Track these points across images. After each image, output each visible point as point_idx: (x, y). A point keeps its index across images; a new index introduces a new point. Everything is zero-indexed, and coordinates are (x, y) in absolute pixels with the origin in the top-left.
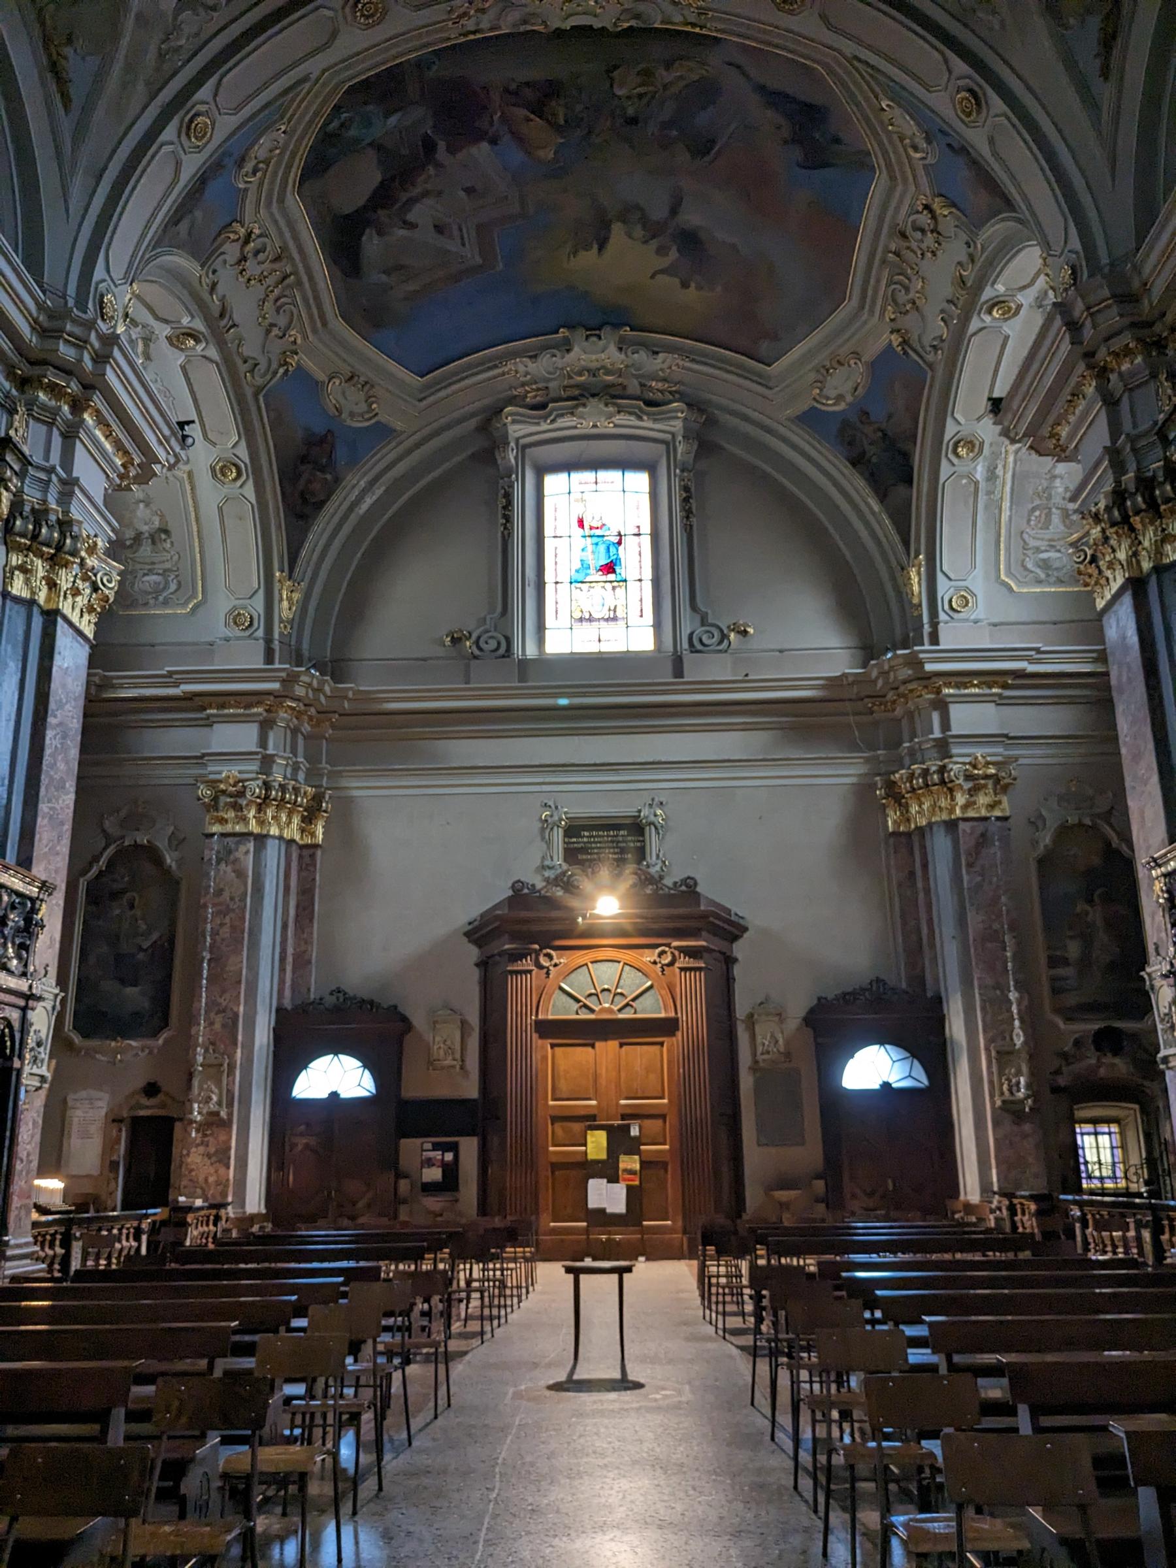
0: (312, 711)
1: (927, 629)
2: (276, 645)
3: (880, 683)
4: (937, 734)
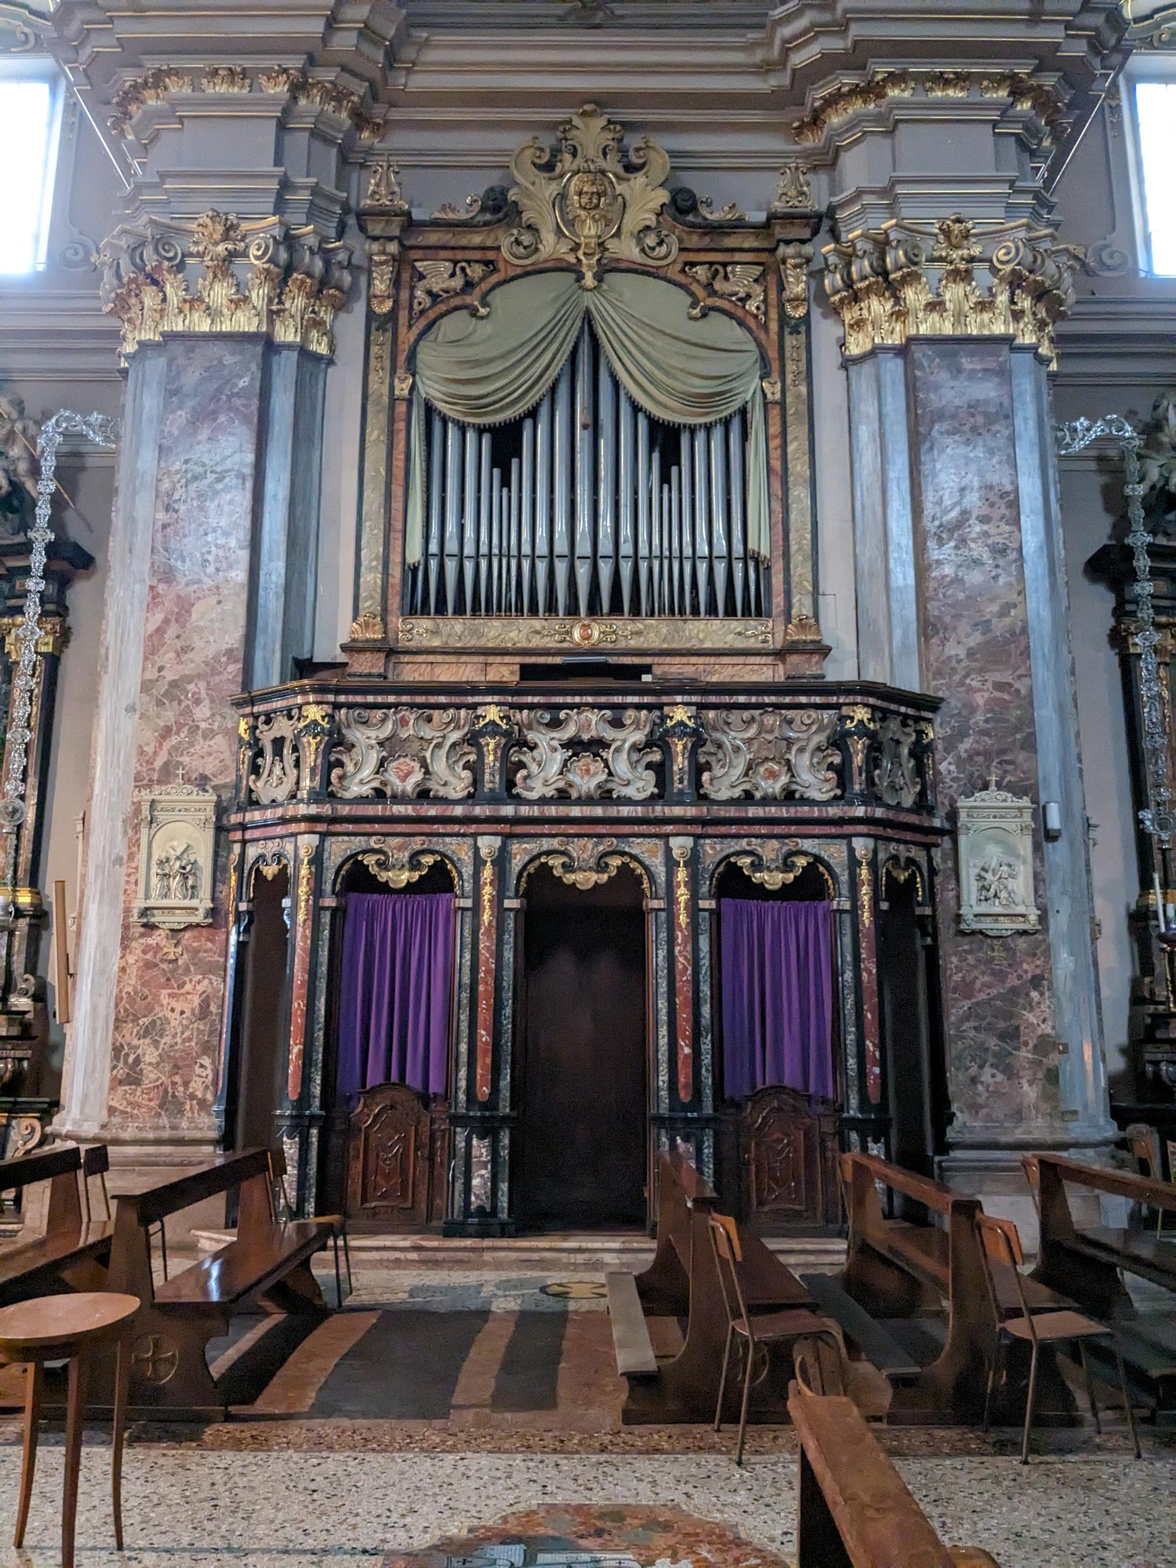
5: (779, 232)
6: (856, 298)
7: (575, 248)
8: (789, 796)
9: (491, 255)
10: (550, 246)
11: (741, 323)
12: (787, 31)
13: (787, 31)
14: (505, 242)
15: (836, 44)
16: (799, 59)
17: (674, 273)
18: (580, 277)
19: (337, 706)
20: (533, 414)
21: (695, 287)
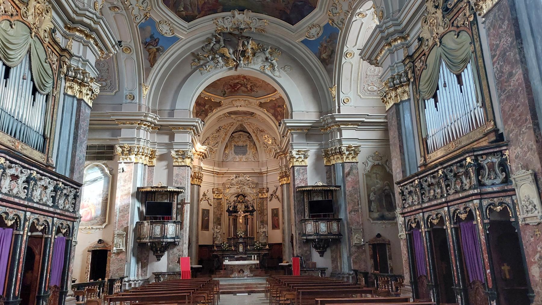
0: (153, 125)
4: (339, 138)
6: (73, 81)
8: (68, 211)
10: (30, 19)
11: (52, 70)
12: (88, 13)
13: (88, 13)
17: (45, 46)
19: (6, 159)
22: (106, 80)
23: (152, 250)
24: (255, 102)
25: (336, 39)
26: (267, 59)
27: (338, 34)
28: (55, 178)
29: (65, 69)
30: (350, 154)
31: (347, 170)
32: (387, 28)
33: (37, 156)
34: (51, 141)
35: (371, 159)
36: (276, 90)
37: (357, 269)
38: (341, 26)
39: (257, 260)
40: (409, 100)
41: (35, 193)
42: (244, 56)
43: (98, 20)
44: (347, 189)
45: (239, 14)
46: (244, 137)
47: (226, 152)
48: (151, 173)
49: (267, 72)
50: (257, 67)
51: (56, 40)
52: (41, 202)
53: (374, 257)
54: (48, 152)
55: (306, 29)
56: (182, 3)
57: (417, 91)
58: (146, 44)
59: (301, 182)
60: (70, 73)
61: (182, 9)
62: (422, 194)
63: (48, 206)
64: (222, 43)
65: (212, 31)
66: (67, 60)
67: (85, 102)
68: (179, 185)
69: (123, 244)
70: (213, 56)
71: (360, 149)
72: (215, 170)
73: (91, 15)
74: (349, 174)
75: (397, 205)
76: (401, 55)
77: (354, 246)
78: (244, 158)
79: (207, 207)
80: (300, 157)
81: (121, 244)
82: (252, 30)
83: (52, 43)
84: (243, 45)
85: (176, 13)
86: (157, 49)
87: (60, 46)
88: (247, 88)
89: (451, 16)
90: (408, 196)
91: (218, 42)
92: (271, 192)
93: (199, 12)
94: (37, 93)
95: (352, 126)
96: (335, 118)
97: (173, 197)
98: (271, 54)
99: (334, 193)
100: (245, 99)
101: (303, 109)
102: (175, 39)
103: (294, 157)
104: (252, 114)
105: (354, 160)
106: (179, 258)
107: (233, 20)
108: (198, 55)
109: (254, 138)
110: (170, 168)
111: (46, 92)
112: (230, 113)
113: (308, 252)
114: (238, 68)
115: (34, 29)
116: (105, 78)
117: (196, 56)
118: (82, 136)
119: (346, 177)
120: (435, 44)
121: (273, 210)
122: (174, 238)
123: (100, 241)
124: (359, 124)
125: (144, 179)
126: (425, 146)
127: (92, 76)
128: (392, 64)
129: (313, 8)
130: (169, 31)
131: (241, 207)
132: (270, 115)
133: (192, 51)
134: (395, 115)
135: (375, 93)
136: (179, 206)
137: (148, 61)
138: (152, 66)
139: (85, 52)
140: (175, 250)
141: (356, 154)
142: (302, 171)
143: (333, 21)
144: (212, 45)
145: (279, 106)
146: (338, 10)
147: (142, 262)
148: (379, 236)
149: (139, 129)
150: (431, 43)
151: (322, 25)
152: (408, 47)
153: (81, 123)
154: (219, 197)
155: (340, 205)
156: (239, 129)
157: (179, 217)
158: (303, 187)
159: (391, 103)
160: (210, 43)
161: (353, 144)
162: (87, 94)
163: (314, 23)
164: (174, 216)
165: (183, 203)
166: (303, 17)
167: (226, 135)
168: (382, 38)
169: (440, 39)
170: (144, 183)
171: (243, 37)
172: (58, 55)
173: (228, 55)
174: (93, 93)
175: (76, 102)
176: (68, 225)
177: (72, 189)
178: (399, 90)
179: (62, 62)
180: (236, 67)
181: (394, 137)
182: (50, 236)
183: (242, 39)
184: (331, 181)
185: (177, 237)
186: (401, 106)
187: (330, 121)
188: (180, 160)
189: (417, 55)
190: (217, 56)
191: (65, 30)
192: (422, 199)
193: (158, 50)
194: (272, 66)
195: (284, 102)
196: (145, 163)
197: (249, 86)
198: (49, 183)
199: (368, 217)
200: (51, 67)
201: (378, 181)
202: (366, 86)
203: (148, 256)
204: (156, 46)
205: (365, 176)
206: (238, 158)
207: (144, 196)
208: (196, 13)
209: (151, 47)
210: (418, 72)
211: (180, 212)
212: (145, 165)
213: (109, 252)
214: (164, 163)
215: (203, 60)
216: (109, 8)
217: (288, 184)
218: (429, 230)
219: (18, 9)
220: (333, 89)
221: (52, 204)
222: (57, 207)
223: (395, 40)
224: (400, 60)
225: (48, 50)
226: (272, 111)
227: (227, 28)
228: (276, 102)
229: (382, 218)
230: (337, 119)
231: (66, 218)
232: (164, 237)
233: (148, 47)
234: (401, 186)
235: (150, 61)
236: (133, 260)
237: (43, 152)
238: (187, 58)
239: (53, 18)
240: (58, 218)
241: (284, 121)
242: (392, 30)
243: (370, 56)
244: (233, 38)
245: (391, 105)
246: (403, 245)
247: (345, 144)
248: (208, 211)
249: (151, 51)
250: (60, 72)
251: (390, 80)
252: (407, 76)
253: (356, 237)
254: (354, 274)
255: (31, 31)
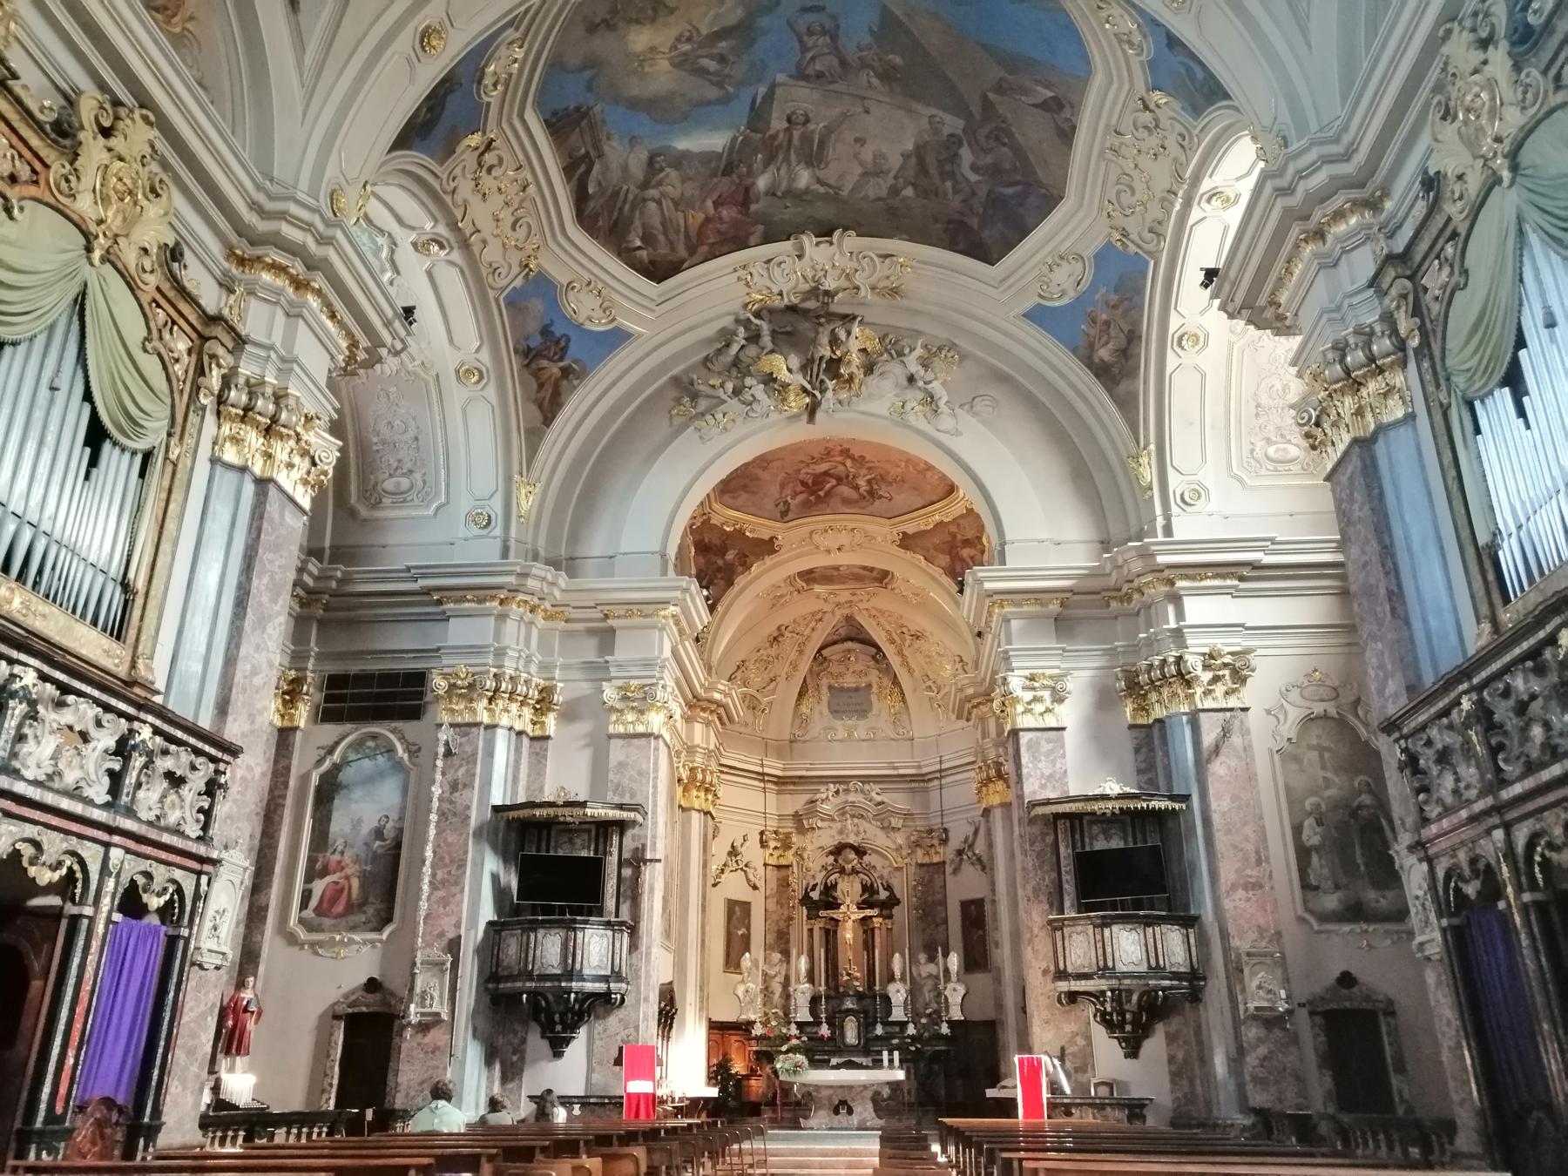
0: (547, 605)
1: (1160, 522)
2: (512, 542)
3: (1114, 575)
4: (1172, 625)
5: (218, 331)
6: (243, 419)
7: (100, 222)
8: (181, 834)
9: (38, 166)
10: (85, 205)
13: (294, 209)
14: (55, 167)
15: (312, 245)
16: (288, 231)
18: (89, 249)
20: (14, 344)
21: (152, 325)
22: (411, 471)
23: (537, 1020)
24: (884, 532)
25: (1140, 291)
26: (911, 379)
27: (1145, 277)
28: (122, 706)
29: (214, 379)
30: (1216, 679)
31: (1208, 739)
32: (1300, 175)
33: (90, 644)
34: (152, 603)
35: (1294, 695)
36: (951, 489)
37: (1267, 1106)
38: (1150, 247)
39: (901, 1067)
40: (1410, 418)
41: (27, 748)
42: (836, 376)
43: (329, 232)
44: (1214, 805)
45: (817, 244)
46: (860, 658)
47: (804, 709)
48: (539, 759)
49: (912, 419)
50: (881, 407)
51: (188, 285)
52: (56, 785)
53: (1333, 1059)
54: (137, 640)
55: (1036, 272)
56: (637, 223)
57: (1438, 376)
58: (529, 356)
59: (1043, 787)
60: (233, 393)
61: (638, 243)
62: (1494, 751)
63: (89, 802)
64: (766, 340)
65: (736, 305)
66: (221, 351)
67: (281, 490)
68: (626, 800)
69: (441, 996)
70: (739, 383)
71: (1254, 661)
72: (767, 770)
73: (304, 214)
74: (1216, 750)
75: (1397, 823)
76: (1364, 263)
77: (1254, 1018)
78: (861, 728)
79: (743, 894)
80: (1036, 699)
81: (436, 994)
82: (863, 293)
83: (171, 294)
84: (834, 341)
85: (619, 255)
86: (562, 369)
87: (199, 306)
88: (857, 488)
89: (1546, 55)
90: (1435, 770)
91: (754, 338)
92: (956, 841)
93: (692, 250)
94: (107, 446)
95: (1217, 582)
96: (1153, 555)
97: (607, 838)
98: (925, 366)
99: (1170, 824)
100: (851, 525)
101: (1043, 537)
102: (617, 338)
103: (1016, 700)
104: (882, 577)
105: (1233, 702)
106: (621, 1049)
107: (798, 265)
108: (692, 384)
109: (894, 661)
110: (600, 744)
111: (142, 445)
112: (809, 576)
113: (1081, 1042)
114: (819, 415)
115: (101, 240)
116: (409, 465)
117: (685, 388)
118: (265, 599)
119: (1209, 761)
120: (1494, 181)
121: (965, 905)
122: (605, 979)
123: (372, 985)
124: (1243, 574)
125: (515, 779)
126: (1491, 577)
127: (310, 408)
128: (1332, 301)
129: (1052, 200)
130: (598, 313)
131: (849, 890)
132: (937, 572)
133: (675, 372)
134: (1359, 481)
135: (1296, 468)
136: (627, 872)
137: (534, 408)
138: (548, 421)
139: (290, 337)
140: (613, 1021)
141: (1239, 677)
142: (1045, 747)
143: (1125, 234)
144: (735, 349)
145: (967, 543)
146: (1138, 196)
147: (505, 1059)
148: (1346, 979)
149: (502, 617)
150: (1474, 185)
151: (1088, 253)
152: (1391, 236)
153: (264, 554)
154: (783, 862)
155: (1194, 867)
156: (843, 632)
157: (625, 909)
158: (1048, 802)
159: (1344, 440)
160: (728, 346)
161: (1227, 644)
162: (290, 466)
163: (1063, 249)
164: (610, 903)
165: (638, 861)
166: (1022, 231)
167: (801, 652)
168: (1289, 217)
169: (1513, 157)
170: (515, 793)
171: (831, 316)
172: (194, 336)
173: (784, 375)
174: (314, 464)
175: (249, 489)
176: (174, 881)
177: (202, 760)
178: (1373, 386)
179: (206, 359)
180: (812, 410)
181: (1366, 564)
182: (88, 911)
183: (828, 322)
184: (1152, 782)
185: (617, 976)
186: (1380, 449)
187: (1137, 566)
188: (630, 717)
189: (1423, 246)
190: (749, 381)
191: (226, 265)
192: (1499, 770)
193: (566, 372)
194: (931, 399)
195: (981, 528)
196: (518, 726)
197: (862, 483)
198: (99, 724)
199: (1300, 911)
200: (165, 368)
201: (1328, 775)
202: (1260, 445)
203: (524, 1041)
204: (561, 359)
205: (1277, 757)
206: (841, 727)
207: (513, 835)
208: (682, 251)
209: (544, 363)
210: (1436, 308)
211: (632, 892)
212: (520, 733)
213: (397, 1022)
214: (583, 727)
215: (708, 396)
216: (414, 245)
217: (1006, 806)
218: (1539, 896)
219: (38, 166)
220: (1144, 460)
221: (109, 798)
222: (130, 812)
223: (1339, 215)
224: (1363, 280)
225: (155, 315)
226: (945, 560)
227: (781, 294)
228: (953, 529)
229: (1355, 912)
230: (1161, 559)
231: (163, 855)
232: (570, 974)
233: (534, 366)
234: (1406, 737)
235: (540, 407)
236: (473, 1054)
237: (118, 633)
238: (658, 394)
239: (177, 215)
240: (128, 851)
241: (974, 574)
242: (1320, 178)
243: (1251, 295)
244: (801, 323)
245: (1341, 448)
246: (1439, 983)
247: (1196, 647)
248: (746, 906)
249: (544, 376)
250: (196, 389)
251: (1330, 356)
252: (1394, 332)
253: (1255, 983)
254: (1260, 1127)
255: (88, 241)
